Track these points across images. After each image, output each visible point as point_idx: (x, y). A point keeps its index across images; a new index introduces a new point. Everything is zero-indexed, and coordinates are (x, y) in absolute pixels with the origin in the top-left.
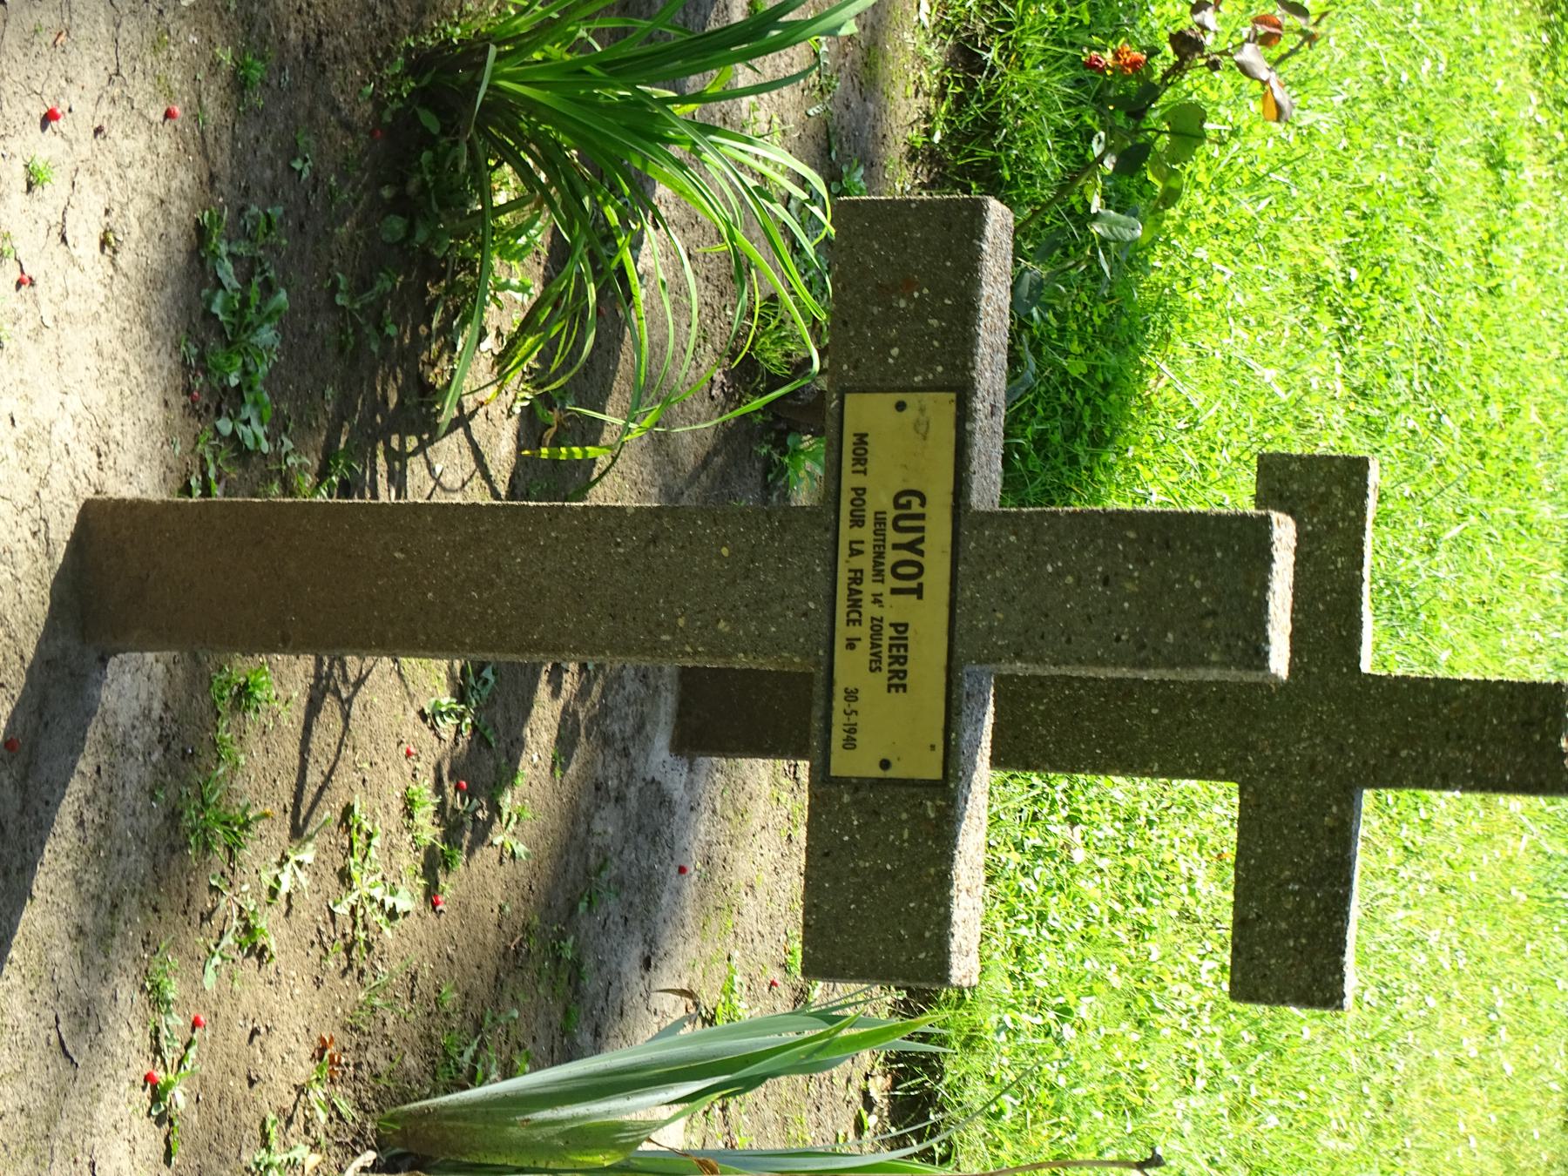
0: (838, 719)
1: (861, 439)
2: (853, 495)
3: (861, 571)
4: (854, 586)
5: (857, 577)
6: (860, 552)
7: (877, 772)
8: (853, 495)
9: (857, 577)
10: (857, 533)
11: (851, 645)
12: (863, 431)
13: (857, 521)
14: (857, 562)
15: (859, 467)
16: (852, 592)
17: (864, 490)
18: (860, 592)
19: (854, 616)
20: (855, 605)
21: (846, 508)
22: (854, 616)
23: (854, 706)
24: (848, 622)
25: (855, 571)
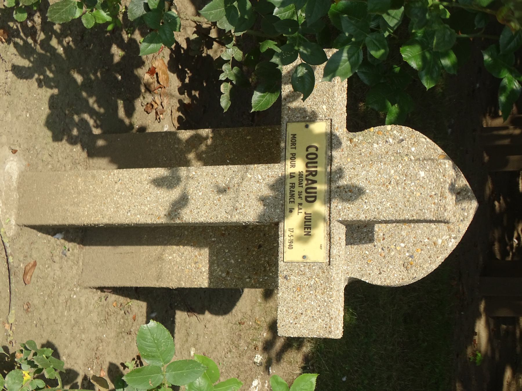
2: (291, 156)
3: (294, 183)
4: (292, 189)
5: (293, 186)
6: (294, 177)
7: (300, 259)
8: (291, 156)
9: (293, 186)
11: (291, 211)
15: (293, 147)
16: (291, 191)
18: (294, 191)
19: (292, 200)
20: (292, 196)
22: (292, 200)
24: (290, 202)
25: (292, 184)
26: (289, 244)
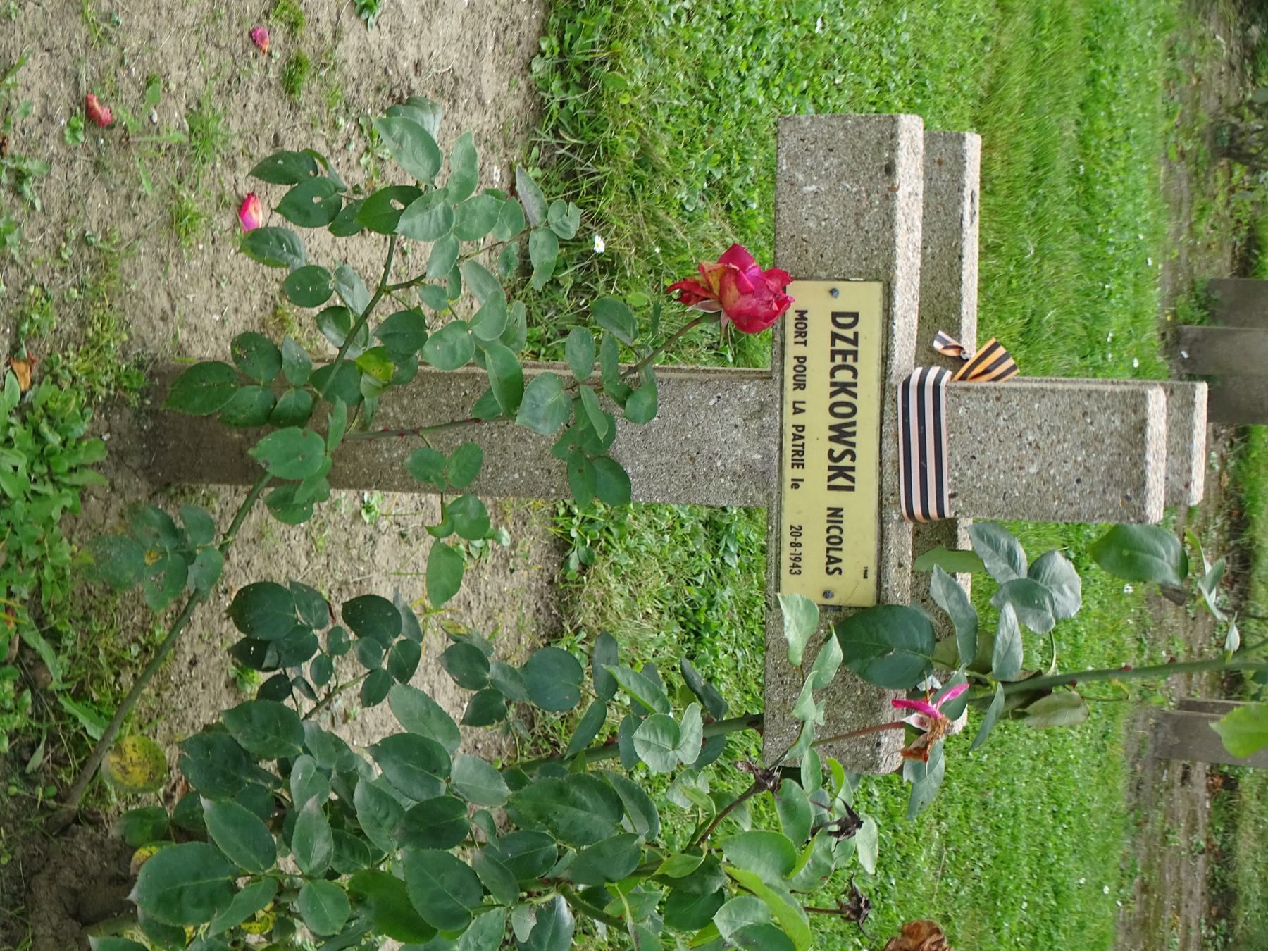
0: (787, 552)
1: (802, 315)
2: (795, 362)
6: (803, 411)
8: (795, 362)
10: (799, 395)
11: (795, 485)
12: (802, 308)
13: (800, 385)
14: (800, 419)
15: (799, 339)
17: (805, 358)
20: (799, 453)
21: (789, 373)
23: (799, 540)
24: (793, 465)
26: (791, 563)
